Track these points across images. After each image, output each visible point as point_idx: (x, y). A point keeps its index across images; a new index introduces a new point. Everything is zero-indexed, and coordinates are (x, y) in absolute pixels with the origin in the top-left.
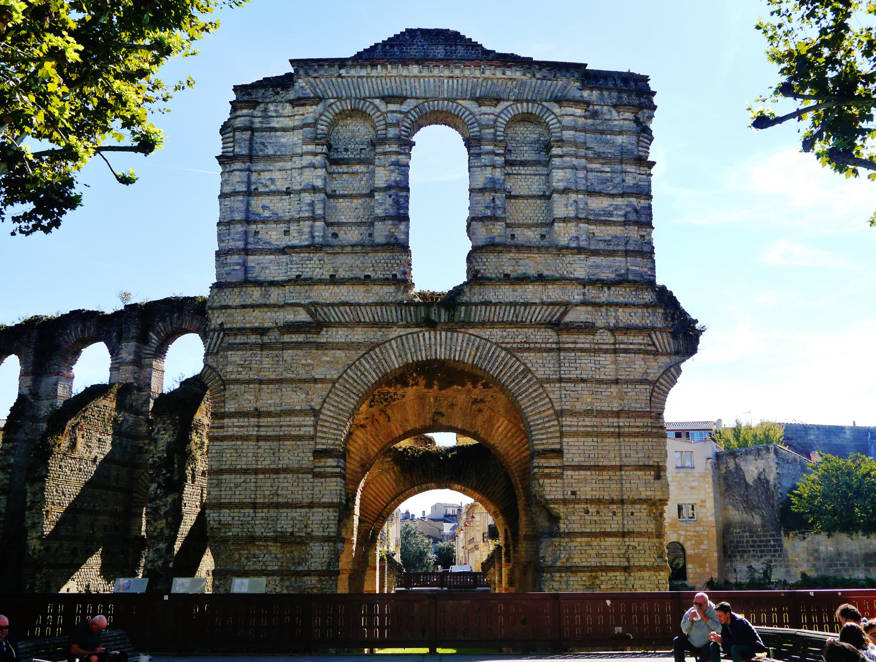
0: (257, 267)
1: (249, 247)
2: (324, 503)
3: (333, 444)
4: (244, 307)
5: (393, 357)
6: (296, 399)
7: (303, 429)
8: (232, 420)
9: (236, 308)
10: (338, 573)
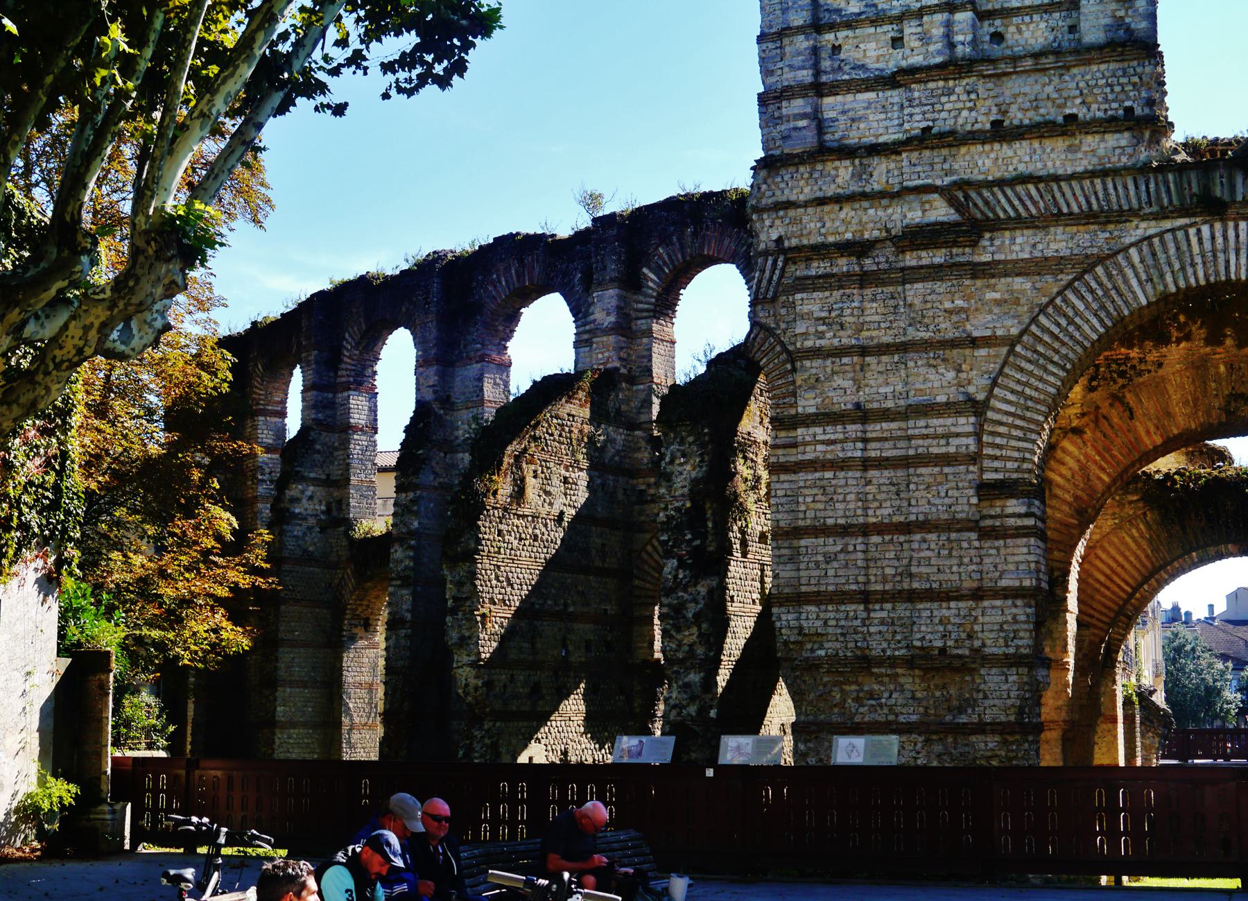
0: (842, 118)
1: (824, 78)
2: (1005, 589)
3: (1018, 470)
4: (821, 202)
5: (1134, 282)
6: (936, 381)
8: (812, 430)
9: (806, 204)
10: (1039, 728)
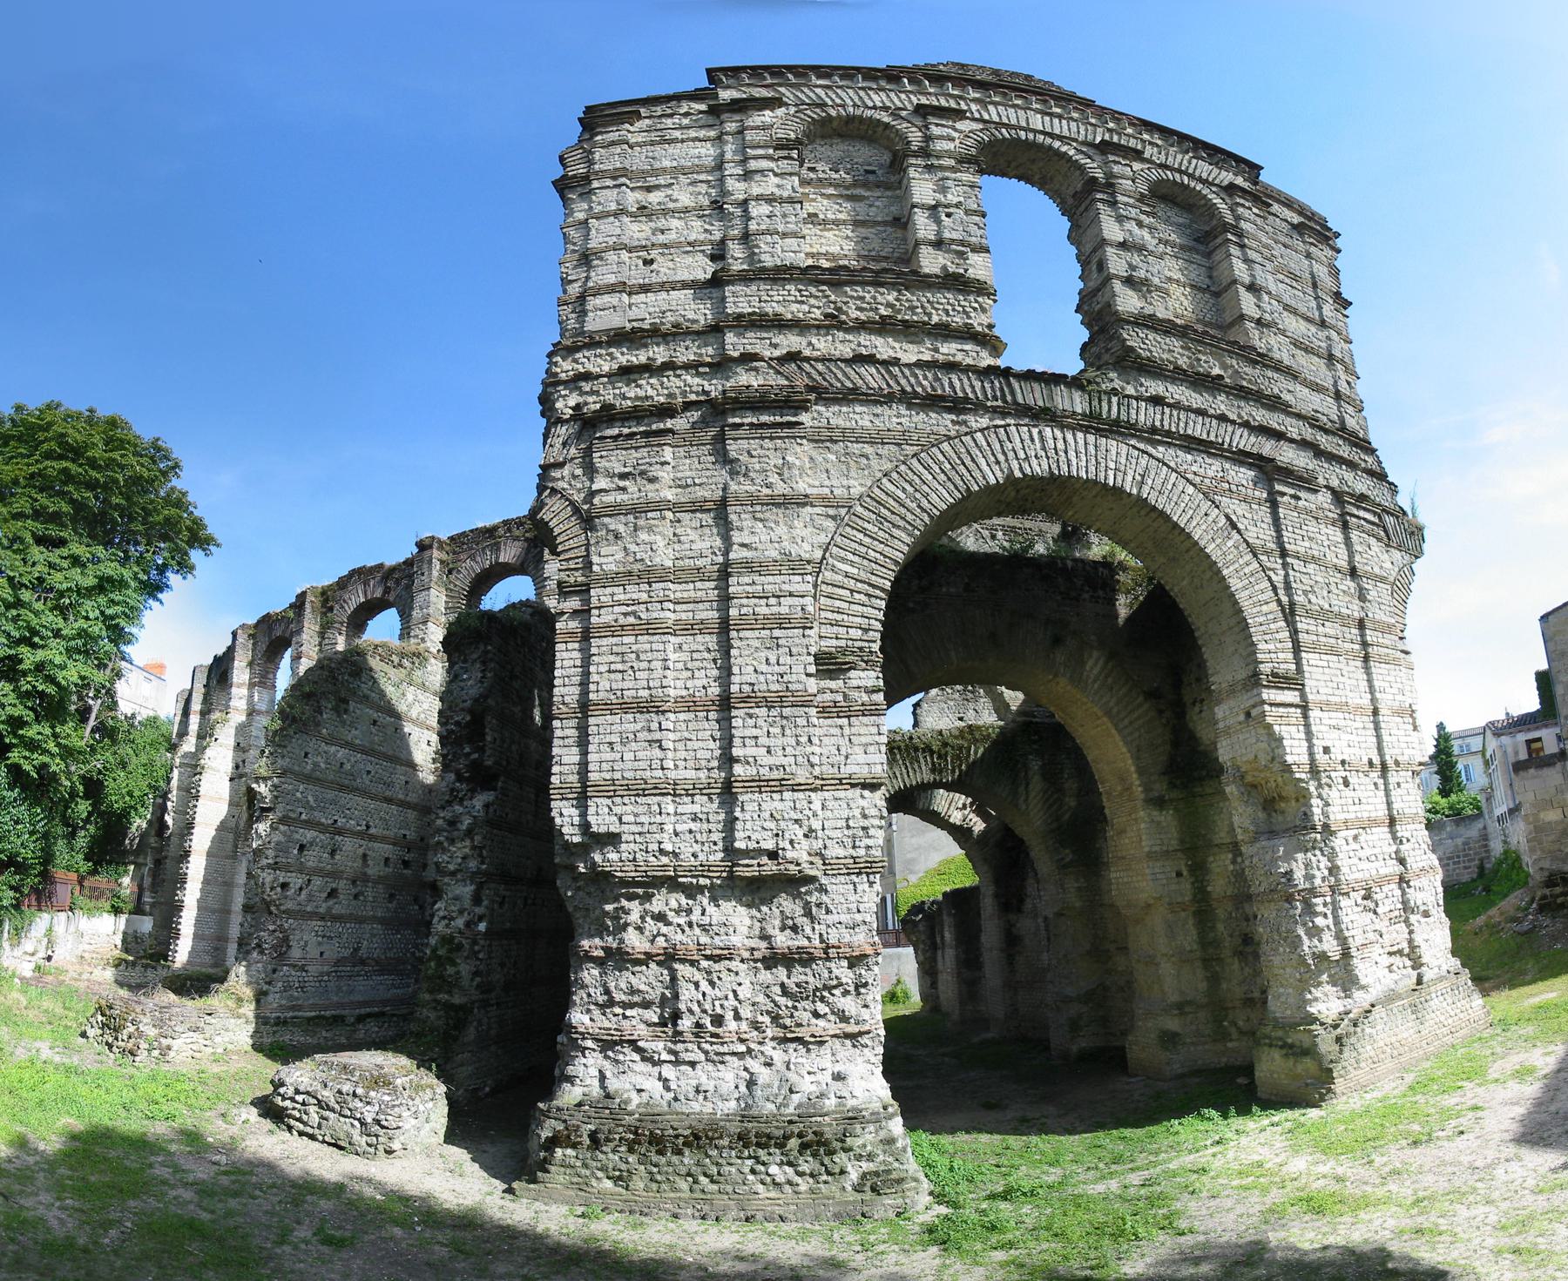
7: (786, 601)
